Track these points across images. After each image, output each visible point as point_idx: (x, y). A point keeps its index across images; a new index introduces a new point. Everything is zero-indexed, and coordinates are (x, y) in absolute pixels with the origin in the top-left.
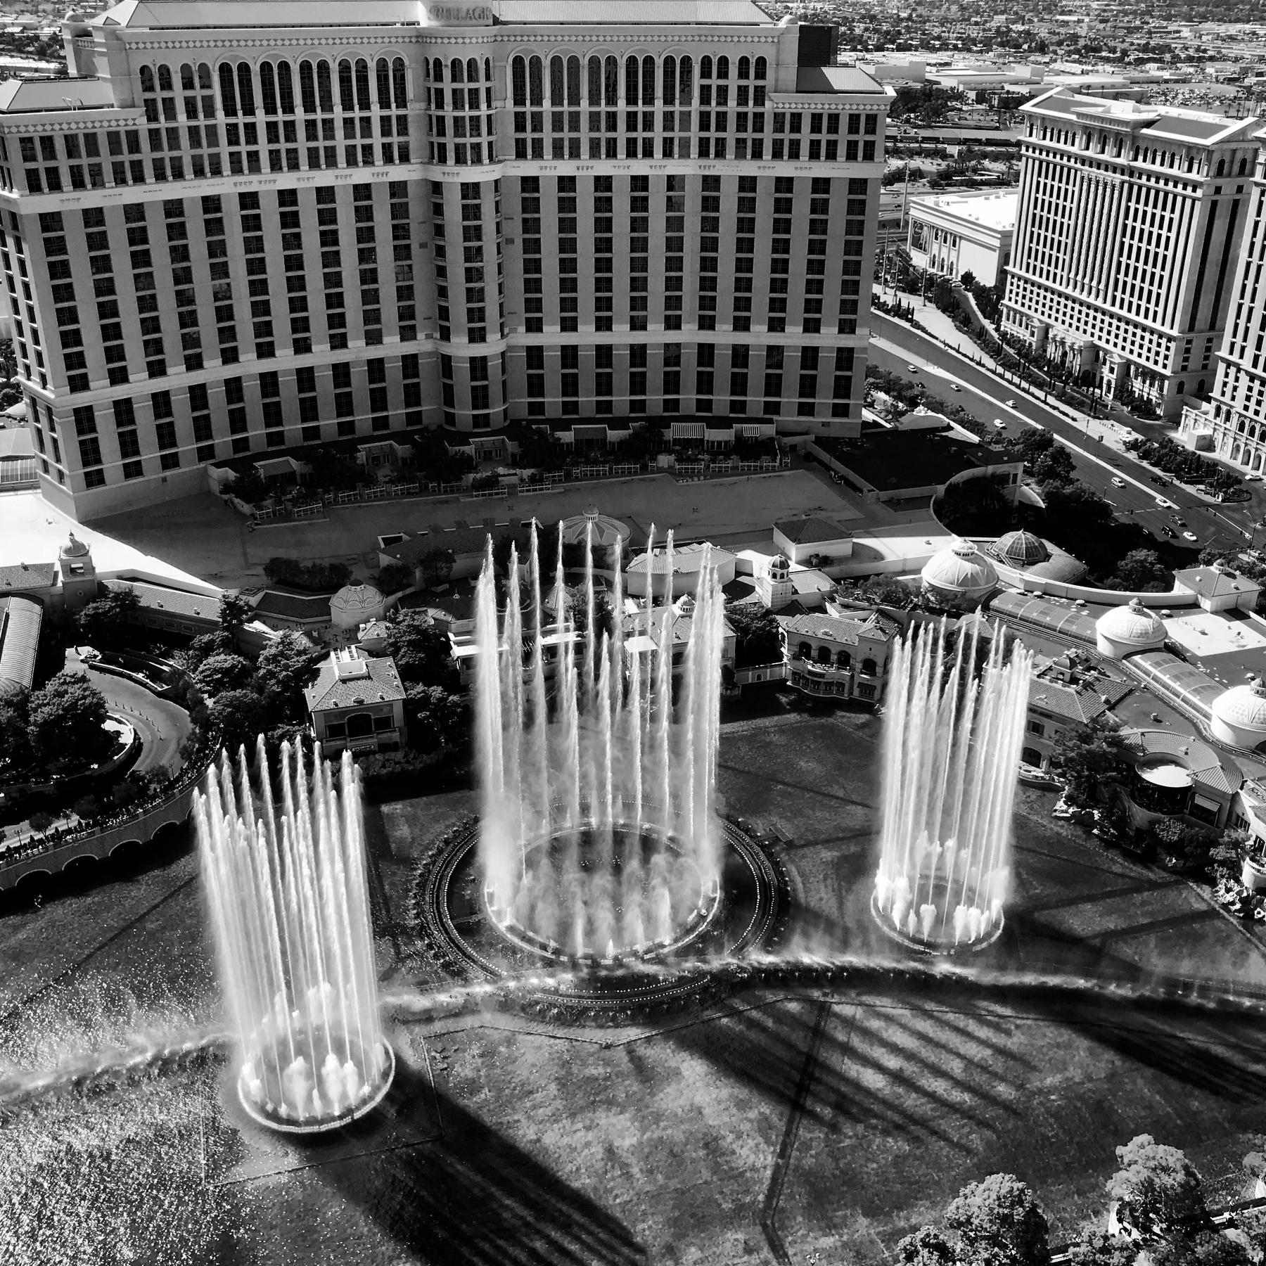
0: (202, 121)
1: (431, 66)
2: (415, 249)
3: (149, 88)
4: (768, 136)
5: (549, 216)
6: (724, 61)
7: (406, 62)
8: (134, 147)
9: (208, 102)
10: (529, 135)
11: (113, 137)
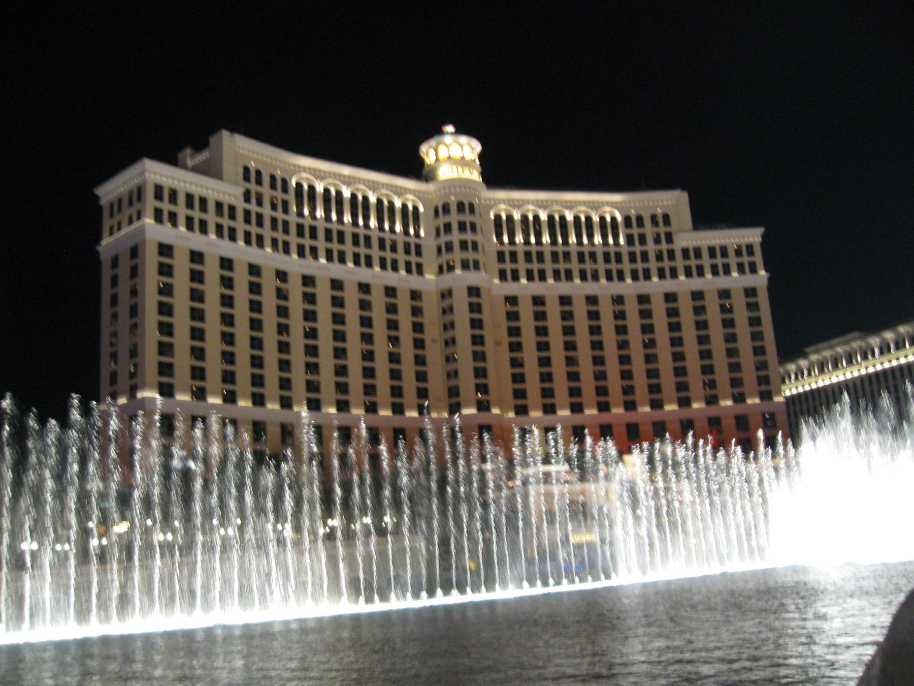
1: (440, 210)
2: (428, 343)
3: (247, 178)
4: (680, 263)
5: (527, 324)
6: (640, 219)
8: (232, 216)
9: (285, 204)
10: (508, 266)
11: (219, 205)
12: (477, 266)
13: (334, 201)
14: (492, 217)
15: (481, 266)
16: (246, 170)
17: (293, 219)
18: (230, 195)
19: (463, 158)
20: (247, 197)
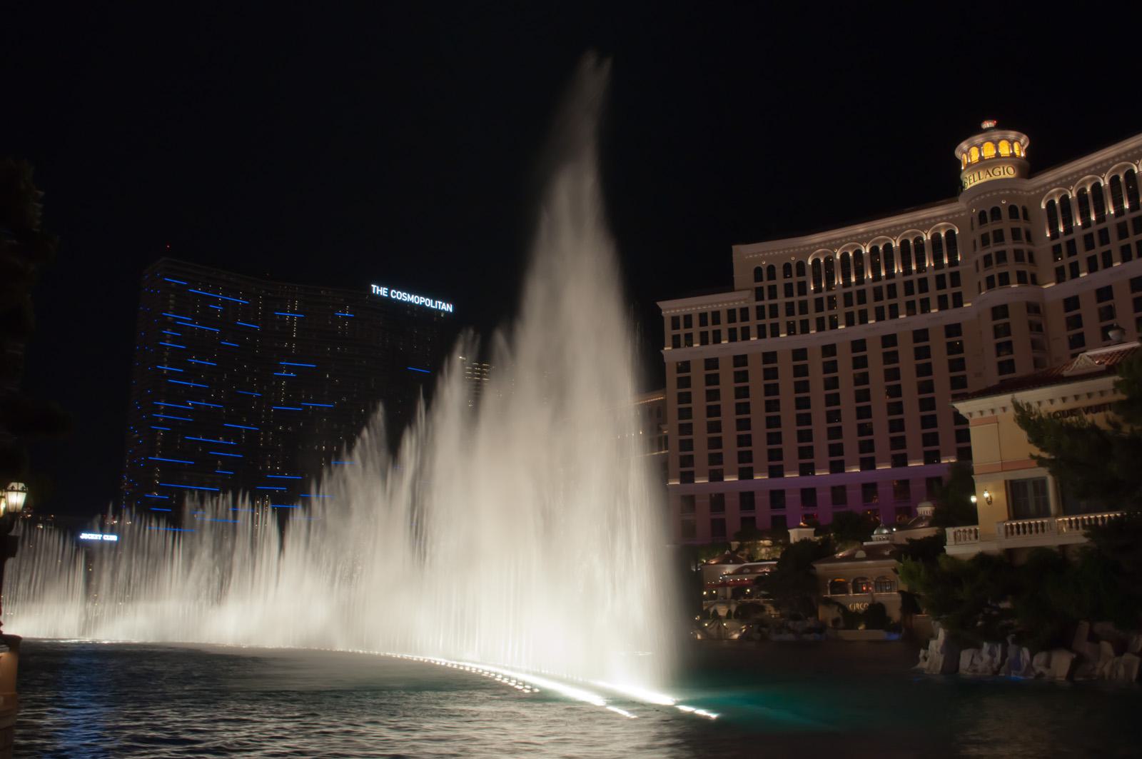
0: (796, 299)
7: (957, 233)
8: (745, 316)
12: (1004, 280)
13: (852, 264)
14: (1043, 206)
15: (1013, 277)
16: (758, 272)
17: (810, 297)
18: (740, 300)
19: (981, 158)
20: (759, 294)
